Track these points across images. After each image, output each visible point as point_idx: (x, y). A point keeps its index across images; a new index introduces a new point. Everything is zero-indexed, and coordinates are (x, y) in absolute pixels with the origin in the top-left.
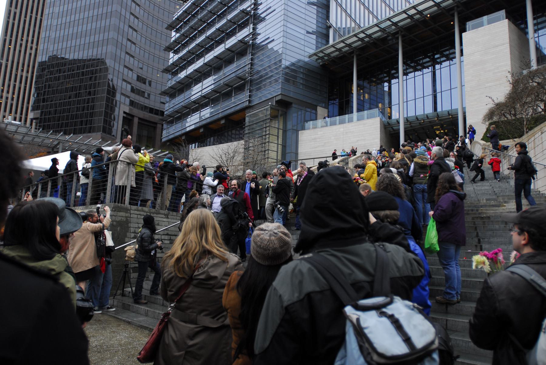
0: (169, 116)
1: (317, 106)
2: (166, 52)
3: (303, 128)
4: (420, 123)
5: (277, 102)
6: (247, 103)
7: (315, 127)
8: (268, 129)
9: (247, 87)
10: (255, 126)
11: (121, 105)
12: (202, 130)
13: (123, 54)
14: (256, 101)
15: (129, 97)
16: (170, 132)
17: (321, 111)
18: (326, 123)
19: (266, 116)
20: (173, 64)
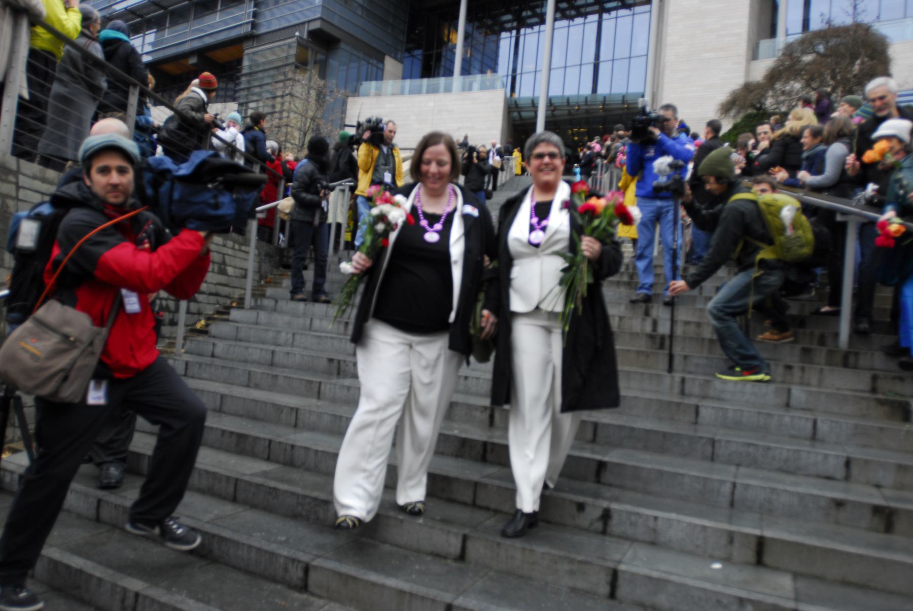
1: (384, 55)
3: (356, 92)
4: (569, 111)
5: (313, 34)
7: (378, 94)
10: (266, 74)
14: (263, 30)
17: (390, 64)
18: (403, 88)
19: (287, 58)
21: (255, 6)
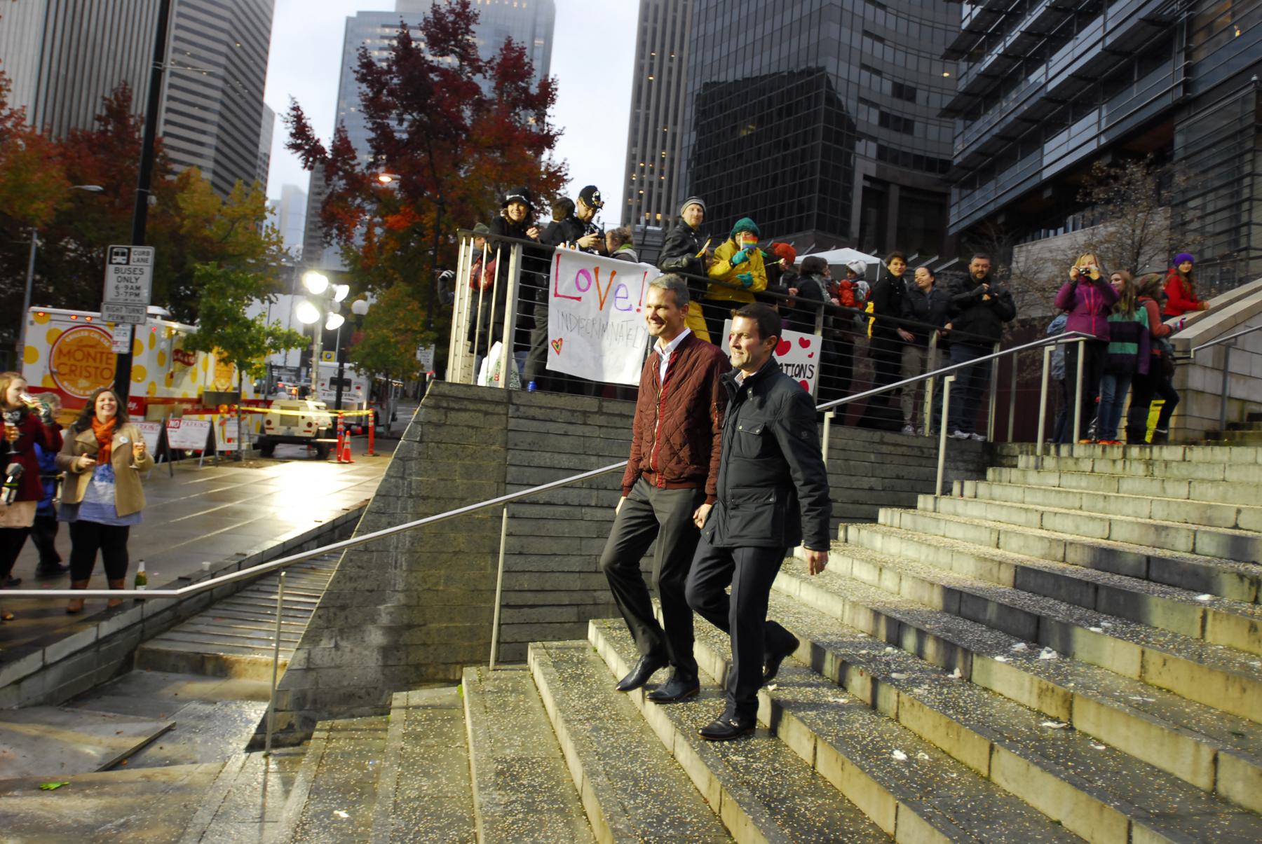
0: (960, 166)
2: (953, 5)
6: (1180, 93)
8: (1249, 157)
9: (1180, 43)
11: (858, 160)
12: (1048, 193)
13: (857, 37)
15: (874, 139)
16: (962, 212)
19: (1241, 119)
20: (969, 30)
21: (1187, 58)
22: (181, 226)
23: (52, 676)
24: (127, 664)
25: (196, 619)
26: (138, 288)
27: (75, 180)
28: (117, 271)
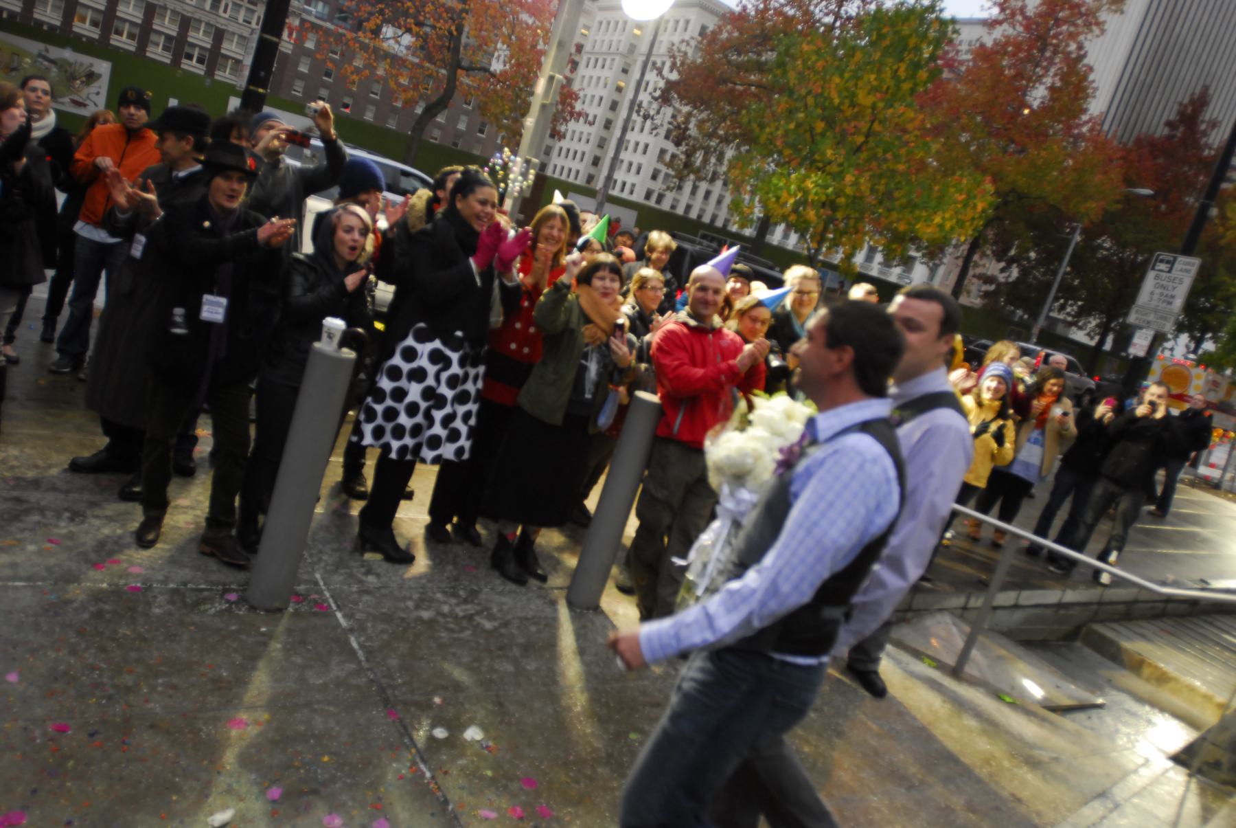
22: (1222, 237)
23: (1018, 616)
24: (1072, 635)
25: (1144, 624)
26: (1173, 297)
27: (1129, 182)
28: (1157, 277)
